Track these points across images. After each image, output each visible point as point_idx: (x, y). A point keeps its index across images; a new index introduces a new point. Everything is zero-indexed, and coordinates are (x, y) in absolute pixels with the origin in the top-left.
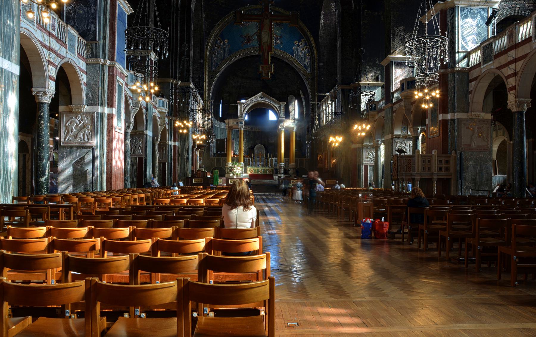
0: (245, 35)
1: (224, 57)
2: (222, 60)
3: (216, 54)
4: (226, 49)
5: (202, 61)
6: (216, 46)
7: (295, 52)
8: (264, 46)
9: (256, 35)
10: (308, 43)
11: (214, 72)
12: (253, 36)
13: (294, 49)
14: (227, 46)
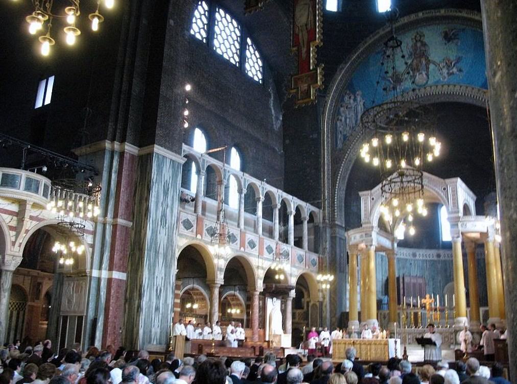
3: (343, 119)
5: (315, 136)
6: (341, 106)
8: (300, 35)
14: (360, 101)
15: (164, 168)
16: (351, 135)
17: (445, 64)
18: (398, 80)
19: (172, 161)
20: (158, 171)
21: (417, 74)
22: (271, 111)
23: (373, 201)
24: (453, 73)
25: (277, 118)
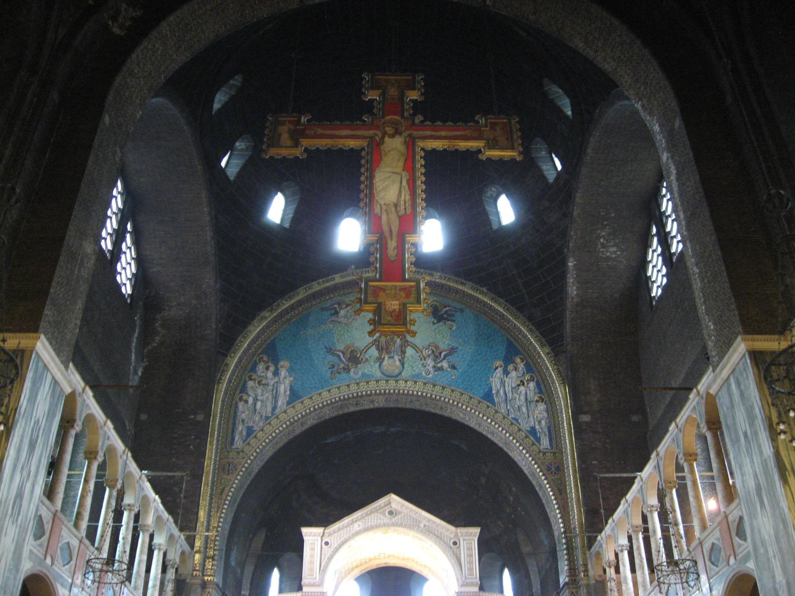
0: (342, 348)
1: (274, 409)
2: (267, 418)
3: (251, 400)
4: (282, 387)
5: (200, 417)
6: (251, 379)
7: (498, 391)
8: (384, 218)
9: (374, 348)
10: (533, 369)
11: (238, 453)
12: (368, 348)
13: (495, 381)
14: (285, 378)
15: (40, 393)
16: (262, 430)
17: (430, 352)
18: (354, 358)
19: (55, 382)
20: (31, 391)
21: (386, 358)
22: (131, 354)
23: (328, 551)
24: (441, 369)
25: (136, 372)
